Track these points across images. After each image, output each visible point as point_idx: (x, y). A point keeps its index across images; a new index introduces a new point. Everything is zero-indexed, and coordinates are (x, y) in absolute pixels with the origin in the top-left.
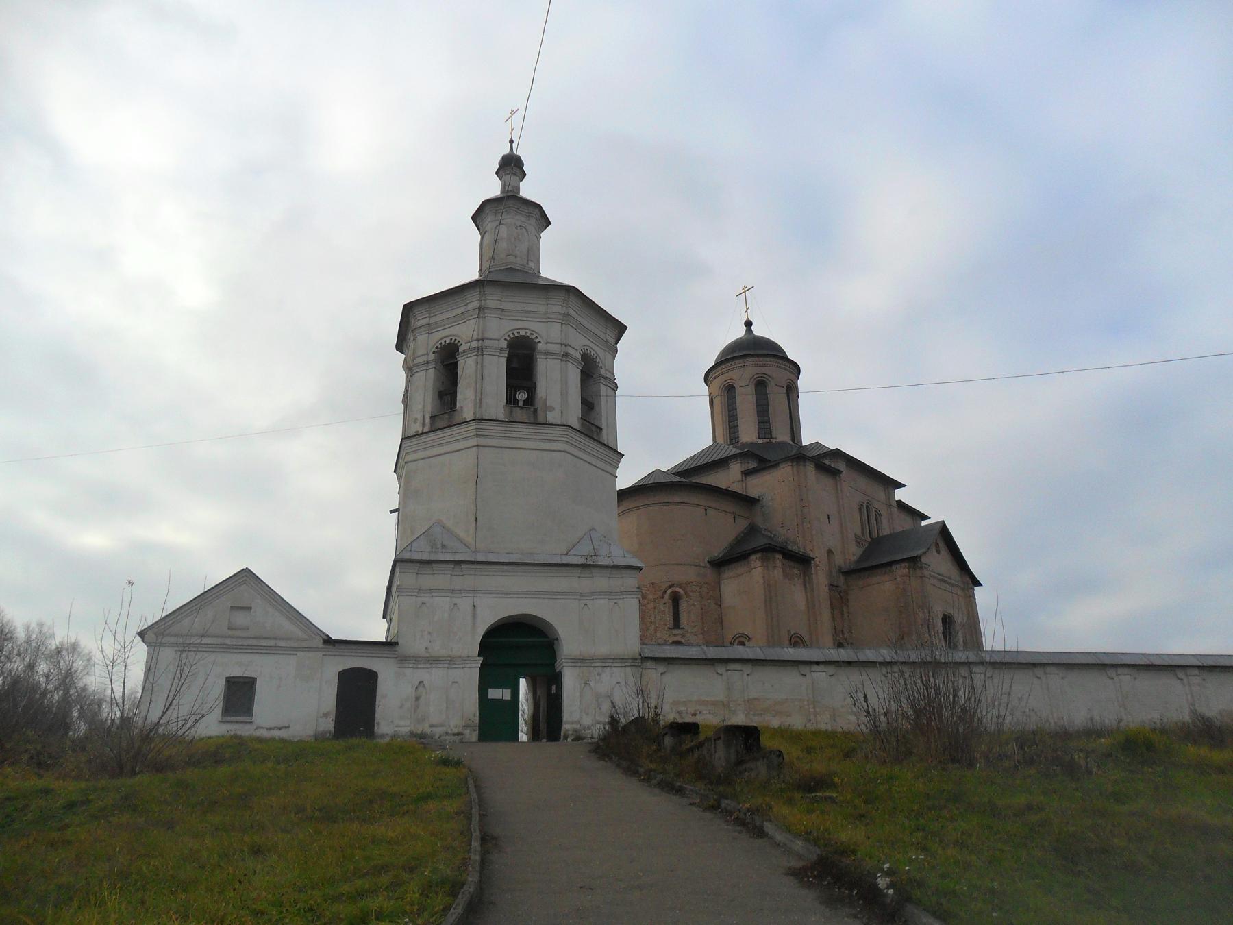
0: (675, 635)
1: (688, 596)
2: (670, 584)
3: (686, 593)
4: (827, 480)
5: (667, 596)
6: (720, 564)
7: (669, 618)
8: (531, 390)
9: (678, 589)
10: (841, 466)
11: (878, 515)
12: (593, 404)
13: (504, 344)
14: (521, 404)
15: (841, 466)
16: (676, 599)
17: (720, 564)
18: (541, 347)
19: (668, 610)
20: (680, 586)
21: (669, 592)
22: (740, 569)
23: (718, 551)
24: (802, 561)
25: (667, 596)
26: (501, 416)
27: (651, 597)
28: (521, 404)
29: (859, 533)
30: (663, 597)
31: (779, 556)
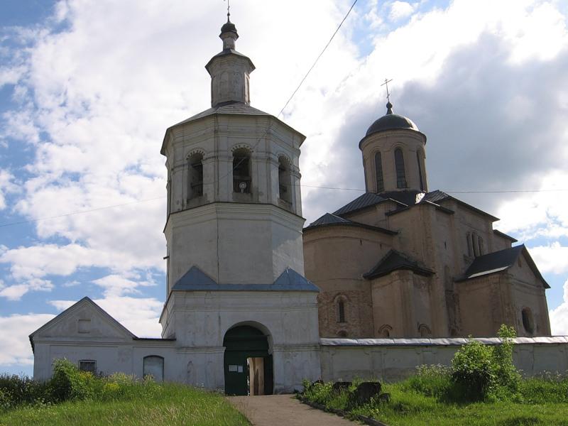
0: (342, 327)
1: (350, 301)
2: (337, 292)
3: (348, 297)
4: (444, 218)
5: (335, 301)
6: (371, 277)
7: (338, 317)
8: (249, 182)
9: (343, 296)
10: (454, 208)
11: (480, 241)
12: (286, 188)
13: (231, 154)
14: (242, 191)
15: (454, 208)
16: (341, 304)
17: (371, 277)
18: (253, 154)
19: (337, 311)
20: (344, 293)
21: (337, 297)
22: (385, 281)
23: (369, 268)
24: (428, 274)
25: (335, 301)
26: (231, 200)
27: (325, 301)
28: (242, 191)
29: (467, 255)
30: (333, 302)
31: (411, 272)
